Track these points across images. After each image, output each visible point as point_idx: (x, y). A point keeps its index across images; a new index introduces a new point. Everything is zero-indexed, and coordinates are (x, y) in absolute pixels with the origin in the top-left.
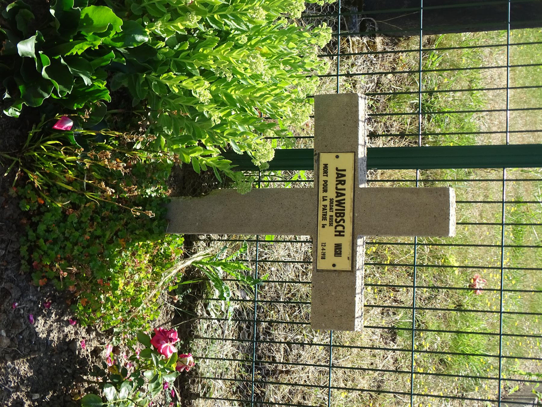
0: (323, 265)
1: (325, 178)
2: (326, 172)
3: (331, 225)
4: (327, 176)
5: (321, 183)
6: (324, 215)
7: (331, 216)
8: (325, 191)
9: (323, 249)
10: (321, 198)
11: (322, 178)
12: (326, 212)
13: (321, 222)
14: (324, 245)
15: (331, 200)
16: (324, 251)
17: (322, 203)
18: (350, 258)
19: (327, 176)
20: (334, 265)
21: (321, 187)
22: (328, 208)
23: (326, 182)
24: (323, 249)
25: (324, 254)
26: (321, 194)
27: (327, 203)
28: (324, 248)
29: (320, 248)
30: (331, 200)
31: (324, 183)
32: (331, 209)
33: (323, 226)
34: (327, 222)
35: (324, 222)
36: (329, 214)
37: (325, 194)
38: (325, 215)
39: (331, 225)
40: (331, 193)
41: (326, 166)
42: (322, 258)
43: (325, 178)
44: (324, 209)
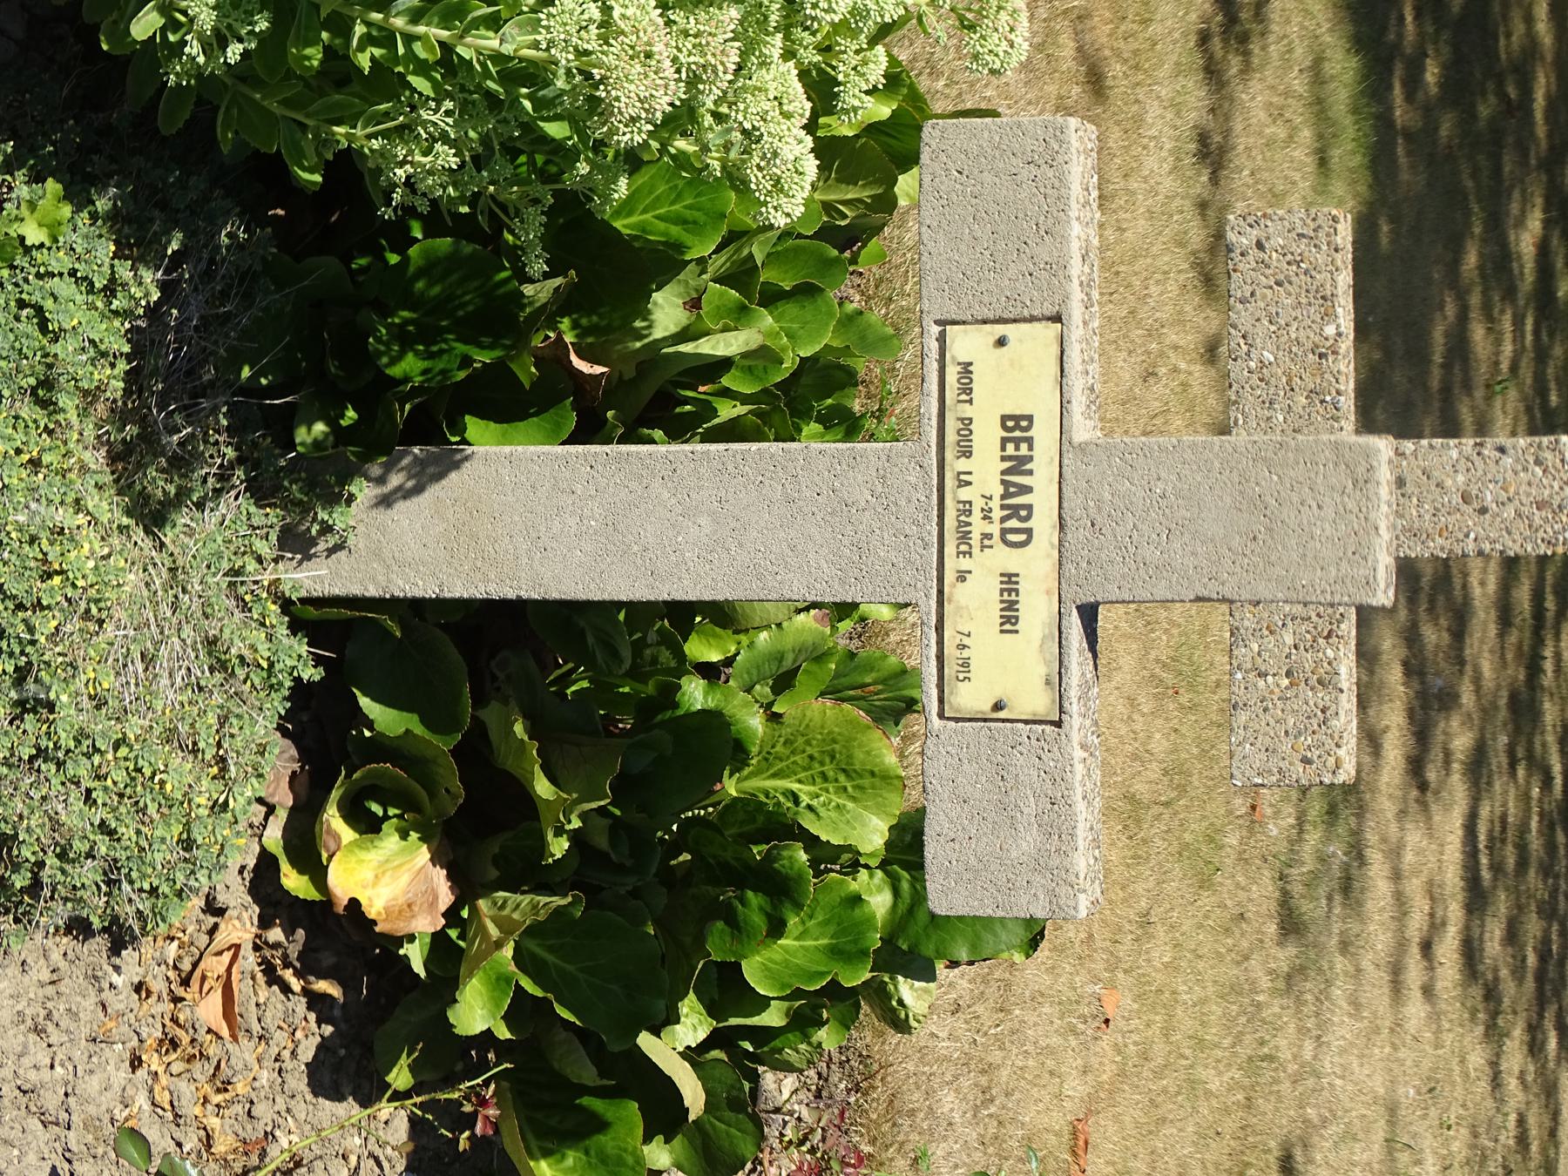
1: (967, 411)
2: (967, 390)
4: (970, 402)
5: (951, 426)
8: (967, 453)
10: (950, 482)
16: (966, 653)
19: (970, 402)
21: (951, 437)
23: (967, 422)
25: (965, 664)
26: (955, 464)
28: (966, 641)
37: (962, 465)
38: (964, 537)
41: (966, 369)
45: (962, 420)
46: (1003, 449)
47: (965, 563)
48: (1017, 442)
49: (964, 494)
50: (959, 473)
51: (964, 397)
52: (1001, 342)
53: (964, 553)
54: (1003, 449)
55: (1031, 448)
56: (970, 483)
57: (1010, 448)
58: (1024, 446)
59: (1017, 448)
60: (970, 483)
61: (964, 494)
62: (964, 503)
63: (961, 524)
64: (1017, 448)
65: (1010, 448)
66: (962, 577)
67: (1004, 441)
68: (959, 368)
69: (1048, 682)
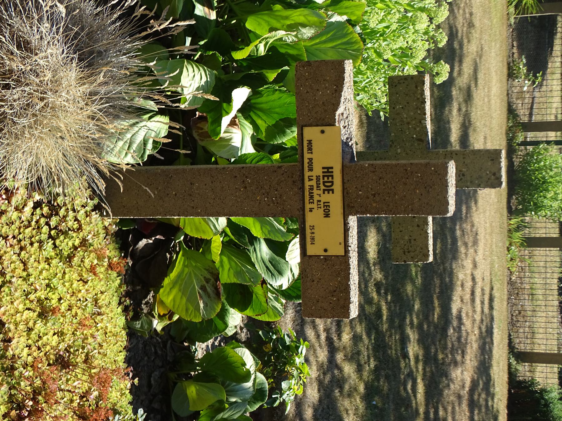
0: (311, 251)
1: (310, 156)
2: (310, 149)
4: (312, 153)
5: (306, 161)
8: (311, 170)
9: (313, 233)
11: (307, 156)
14: (313, 227)
16: (313, 235)
17: (307, 184)
18: (342, 241)
19: (312, 153)
20: (326, 250)
22: (315, 187)
23: (311, 160)
24: (313, 233)
25: (313, 239)
26: (307, 174)
27: (314, 183)
28: (313, 231)
29: (308, 231)
31: (308, 161)
37: (310, 173)
38: (311, 197)
41: (310, 142)
42: (311, 244)
43: (310, 156)
44: (310, 189)
46: (323, 179)
47: (311, 206)
48: (328, 177)
49: (311, 183)
51: (309, 151)
52: (323, 132)
53: (311, 203)
54: (323, 179)
55: (332, 179)
56: (312, 180)
57: (326, 179)
58: (330, 178)
59: (328, 179)
60: (312, 180)
61: (311, 183)
62: (311, 186)
63: (310, 193)
64: (328, 179)
65: (326, 179)
66: (311, 210)
67: (324, 176)
68: (307, 142)
69: (340, 244)
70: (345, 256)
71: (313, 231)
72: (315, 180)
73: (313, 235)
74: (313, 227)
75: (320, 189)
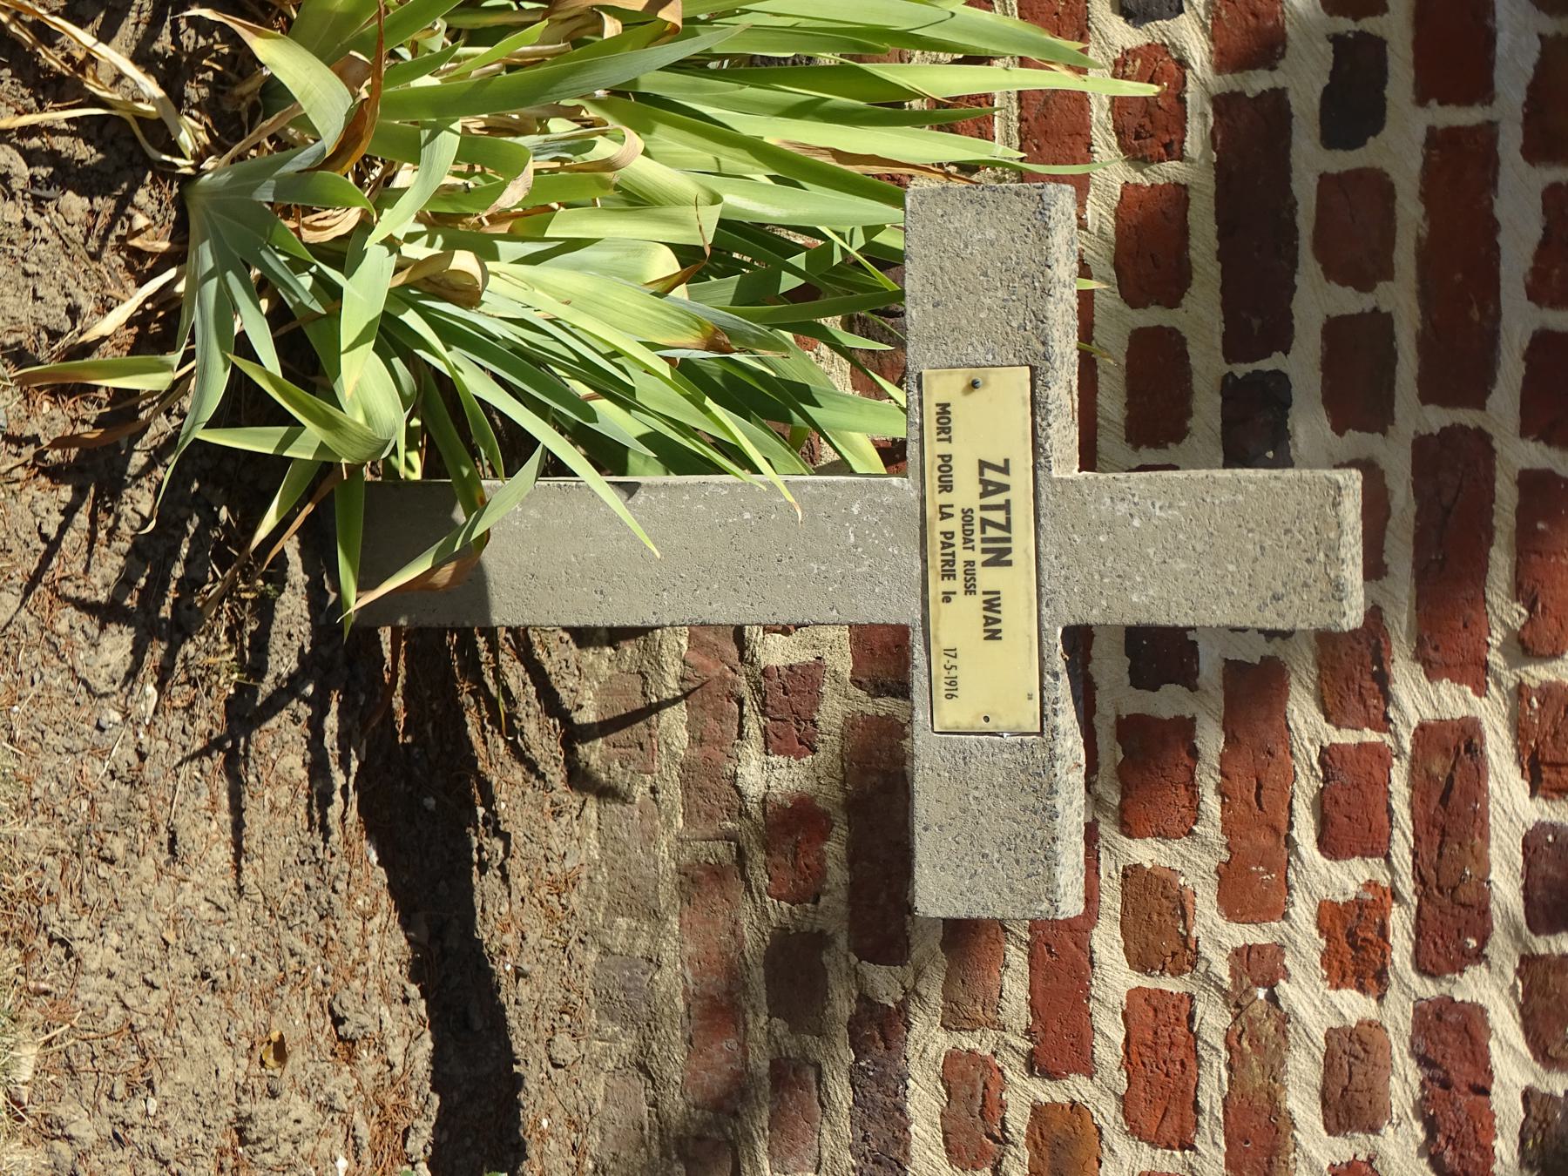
1: (944, 448)
2: (944, 429)
3: (970, 590)
4: (949, 440)
6: (946, 562)
7: (970, 563)
8: (946, 487)
11: (934, 448)
12: (953, 554)
13: (937, 586)
15: (967, 514)
16: (953, 673)
17: (937, 527)
19: (949, 440)
20: (987, 719)
22: (958, 540)
23: (946, 459)
25: (953, 683)
26: (935, 499)
27: (955, 524)
28: (953, 661)
30: (967, 514)
32: (967, 540)
33: (947, 597)
34: (958, 585)
35: (948, 585)
36: (962, 556)
37: (944, 498)
39: (970, 590)
40: (966, 493)
41: (944, 409)
42: (950, 696)
43: (944, 448)
44: (945, 545)
45: (942, 457)
46: (983, 531)
50: (941, 507)
51: (943, 436)
54: (983, 531)
56: (951, 516)
60: (951, 516)
68: (938, 409)
69: (1030, 697)
70: (1041, 734)
71: (953, 661)
72: (958, 515)
73: (953, 673)
74: (951, 653)
75: (973, 548)
